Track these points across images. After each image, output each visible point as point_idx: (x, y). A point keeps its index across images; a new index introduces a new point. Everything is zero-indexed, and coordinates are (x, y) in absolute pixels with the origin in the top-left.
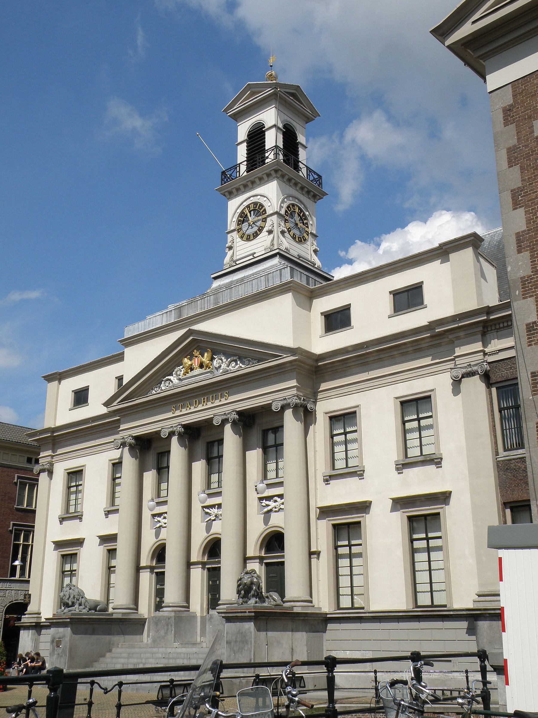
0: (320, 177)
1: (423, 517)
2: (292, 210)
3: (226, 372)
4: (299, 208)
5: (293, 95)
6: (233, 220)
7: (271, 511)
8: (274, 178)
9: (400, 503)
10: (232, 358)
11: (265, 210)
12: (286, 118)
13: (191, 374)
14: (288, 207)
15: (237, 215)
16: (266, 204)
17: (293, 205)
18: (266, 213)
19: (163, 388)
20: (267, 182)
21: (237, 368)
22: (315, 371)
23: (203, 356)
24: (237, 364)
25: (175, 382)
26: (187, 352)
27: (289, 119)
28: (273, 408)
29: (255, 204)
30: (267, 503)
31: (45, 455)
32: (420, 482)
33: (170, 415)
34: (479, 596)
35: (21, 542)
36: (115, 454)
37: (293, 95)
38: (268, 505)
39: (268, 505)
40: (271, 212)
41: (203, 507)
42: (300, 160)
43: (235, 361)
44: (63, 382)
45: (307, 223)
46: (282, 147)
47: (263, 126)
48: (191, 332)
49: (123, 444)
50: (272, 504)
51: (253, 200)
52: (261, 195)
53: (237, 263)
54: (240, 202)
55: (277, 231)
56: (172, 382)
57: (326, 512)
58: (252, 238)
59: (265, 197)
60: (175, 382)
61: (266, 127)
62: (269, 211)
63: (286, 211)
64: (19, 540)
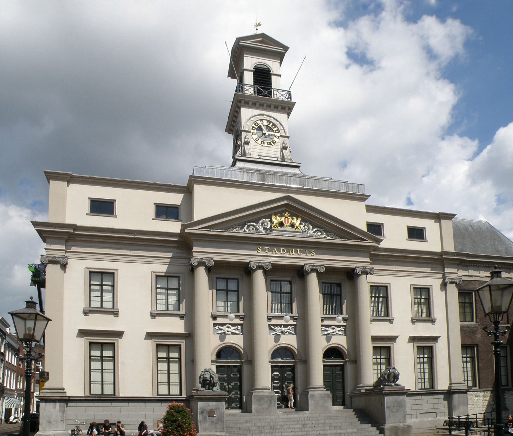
1: (425, 348)
3: (311, 236)
7: (330, 334)
8: (286, 112)
9: (413, 339)
10: (319, 229)
13: (280, 229)
19: (247, 230)
20: (279, 112)
21: (322, 237)
23: (293, 219)
24: (322, 234)
25: (259, 229)
26: (279, 211)
30: (327, 329)
32: (423, 330)
33: (254, 253)
38: (327, 331)
39: (327, 331)
40: (284, 135)
41: (269, 325)
43: (321, 231)
44: (72, 185)
50: (330, 330)
52: (274, 118)
53: (261, 157)
54: (254, 114)
56: (257, 229)
58: (266, 144)
59: (277, 121)
60: (259, 229)
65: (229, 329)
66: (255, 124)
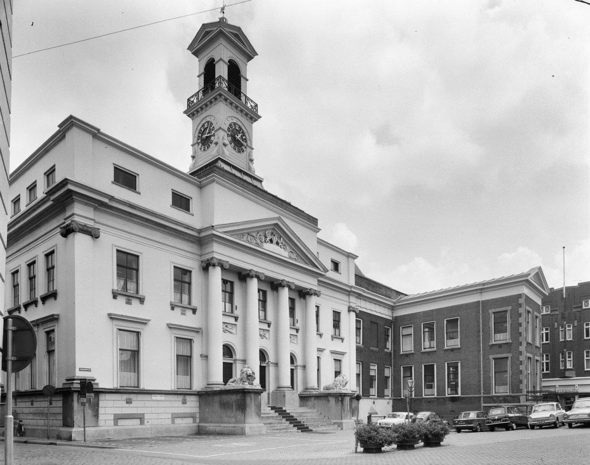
0: (256, 105)
2: (234, 127)
4: (240, 127)
5: (236, 36)
11: (213, 127)
12: (231, 55)
14: (230, 125)
17: (235, 124)
27: (234, 56)
37: (236, 36)
45: (245, 139)
46: (227, 79)
47: (214, 60)
61: (216, 61)
63: (228, 128)
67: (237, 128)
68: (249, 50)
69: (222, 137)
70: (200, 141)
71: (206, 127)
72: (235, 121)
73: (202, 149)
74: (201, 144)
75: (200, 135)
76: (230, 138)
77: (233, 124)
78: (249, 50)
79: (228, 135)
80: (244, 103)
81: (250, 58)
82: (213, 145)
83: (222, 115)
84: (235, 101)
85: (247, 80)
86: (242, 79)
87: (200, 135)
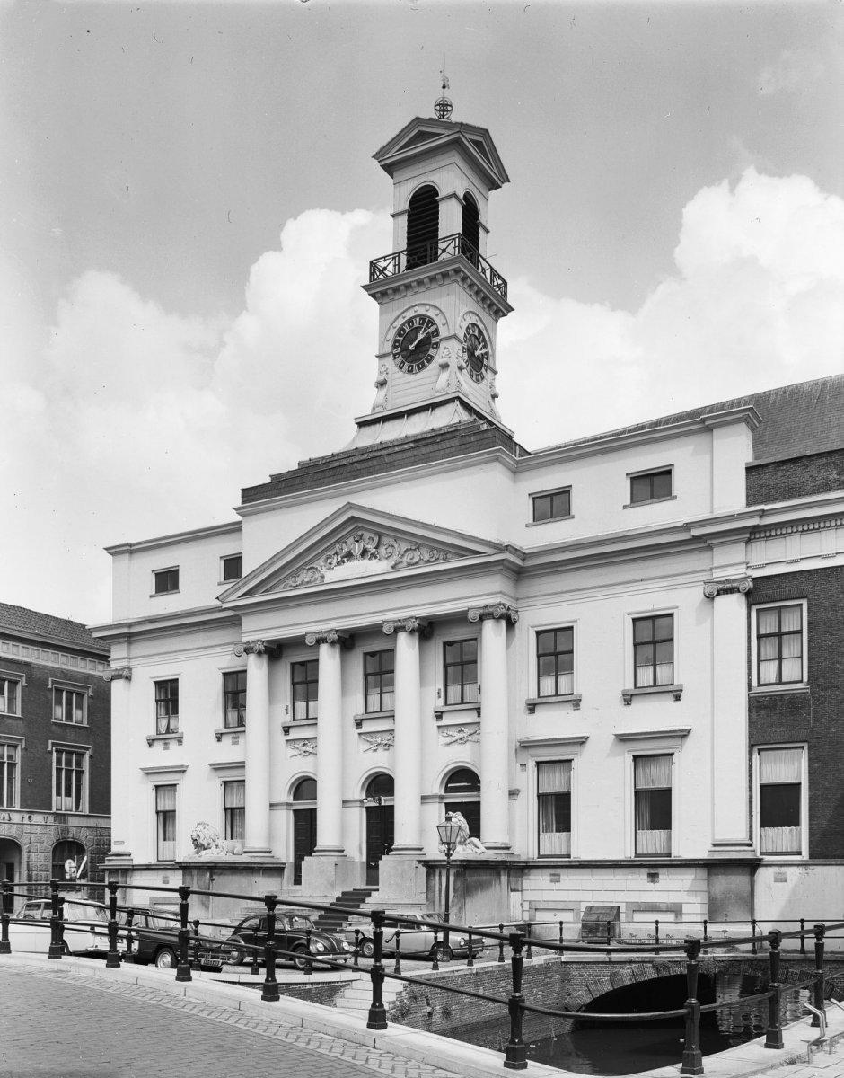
4: (480, 331)
6: (388, 337)
15: (393, 332)
16: (439, 321)
18: (438, 335)
22: (522, 569)
28: (470, 616)
29: (423, 318)
31: (118, 653)
34: (715, 845)
35: (74, 767)
36: (228, 661)
40: (447, 335)
42: (480, 252)
48: (350, 506)
49: (248, 651)
51: (421, 311)
55: (453, 365)
57: (526, 746)
62: (443, 333)
64: (71, 766)
65: (304, 748)
66: (399, 335)
67: (476, 334)
68: (495, 171)
69: (450, 352)
70: (399, 350)
71: (416, 325)
72: (474, 319)
73: (406, 367)
74: (401, 357)
75: (401, 339)
76: (466, 355)
77: (470, 327)
78: (495, 171)
79: (464, 348)
80: (489, 281)
81: (493, 185)
82: (433, 367)
83: (452, 309)
84: (472, 274)
85: (487, 231)
86: (481, 230)
87: (401, 339)
